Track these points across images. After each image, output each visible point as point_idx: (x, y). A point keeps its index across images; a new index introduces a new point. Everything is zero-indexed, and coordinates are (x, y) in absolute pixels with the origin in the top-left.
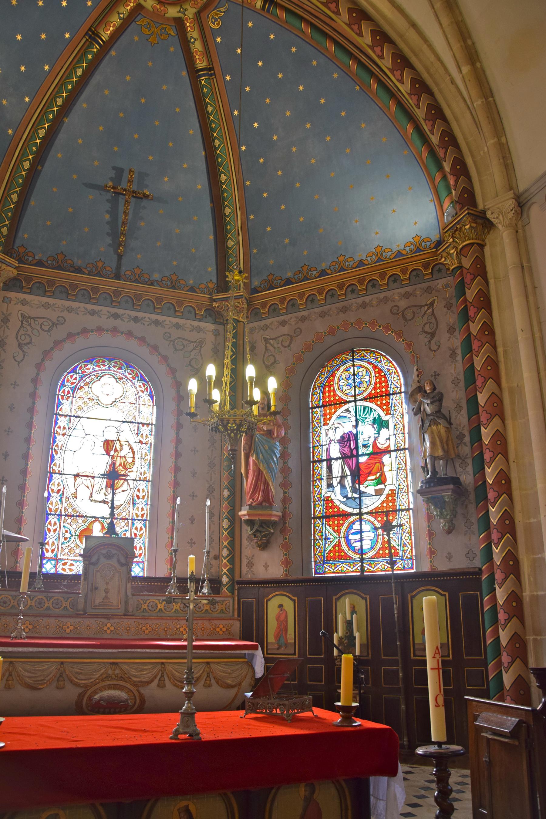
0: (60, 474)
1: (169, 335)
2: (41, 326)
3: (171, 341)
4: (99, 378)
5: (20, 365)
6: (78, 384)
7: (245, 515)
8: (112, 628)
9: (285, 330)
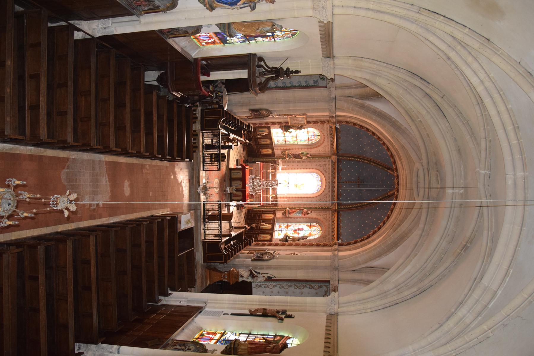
9: (328, 218)
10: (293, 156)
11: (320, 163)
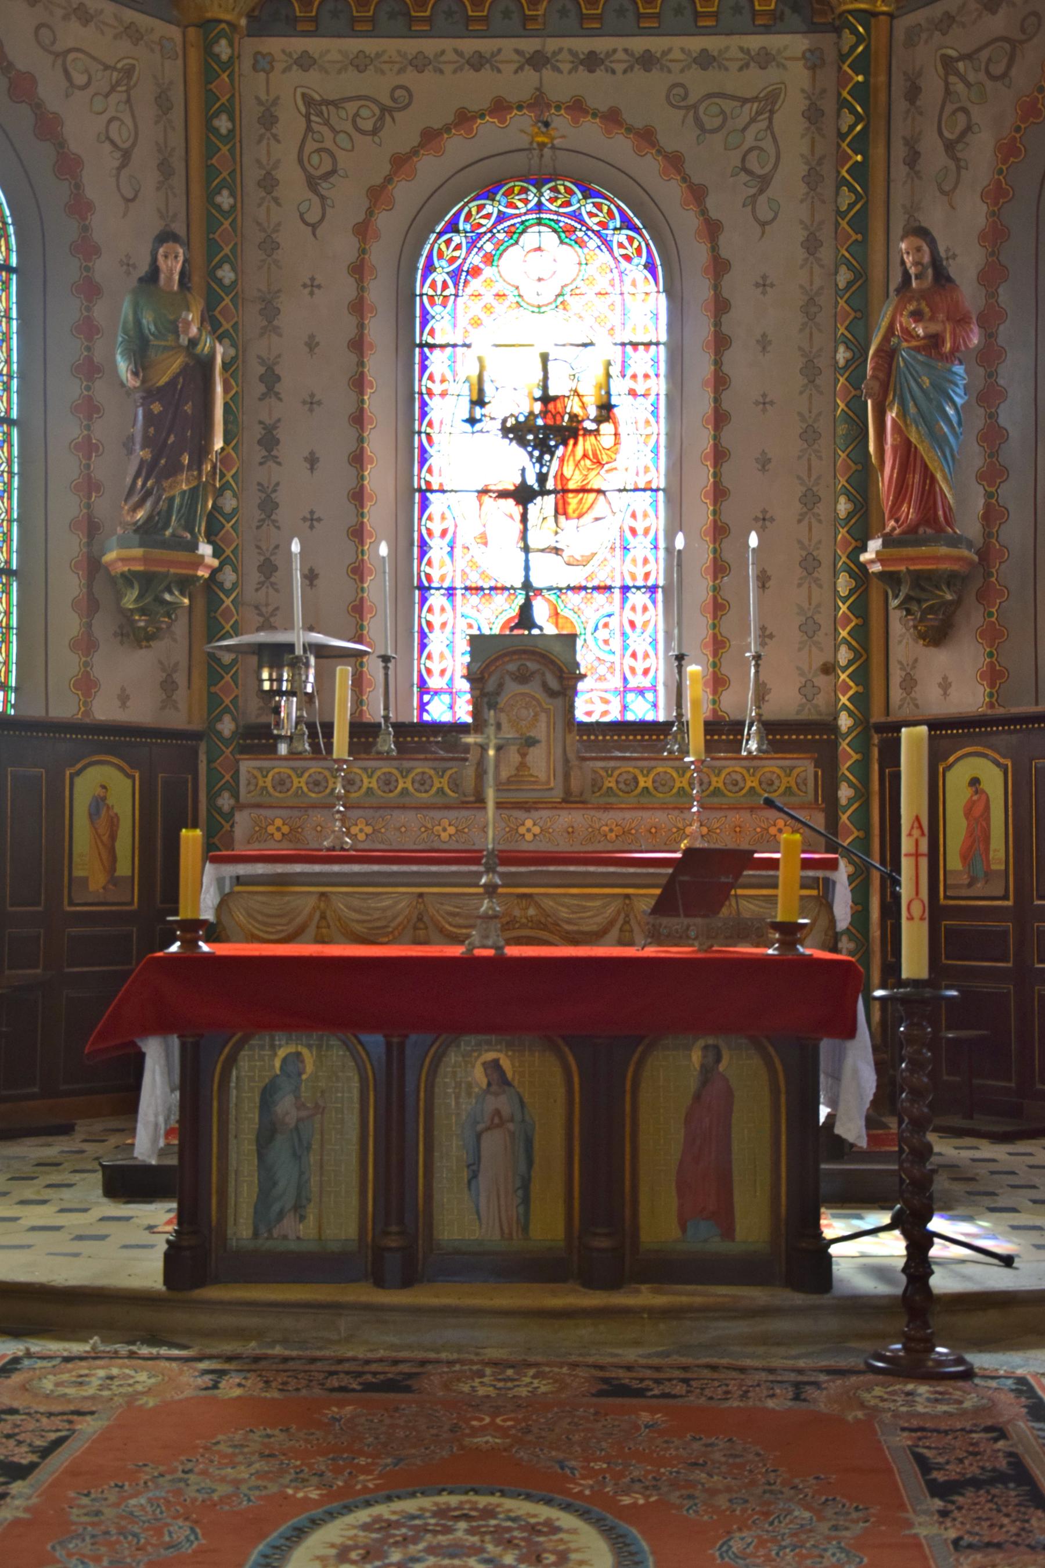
0: (443, 491)
1: (681, 91)
2: (354, 122)
3: (687, 108)
4: (515, 236)
5: (318, 232)
6: (465, 259)
7: (872, 562)
8: (536, 830)
10: (174, 469)
11: (290, 175)
